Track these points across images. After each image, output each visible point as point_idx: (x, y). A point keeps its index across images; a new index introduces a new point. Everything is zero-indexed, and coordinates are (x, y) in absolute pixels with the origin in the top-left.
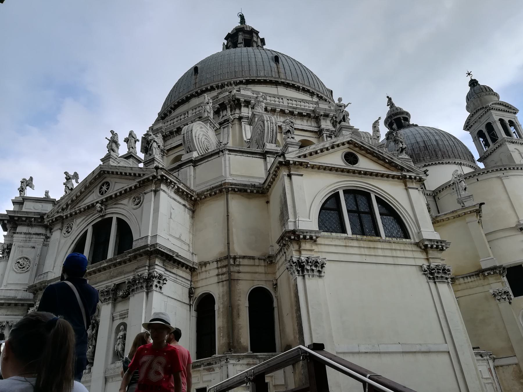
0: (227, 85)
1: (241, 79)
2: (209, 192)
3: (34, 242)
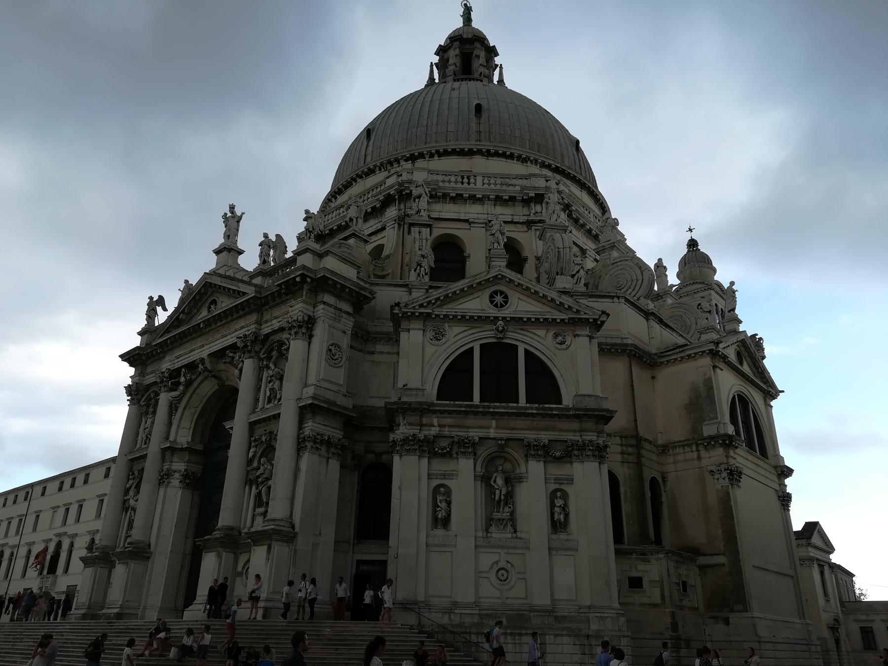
0: (531, 162)
1: (552, 162)
2: (608, 347)
3: (343, 323)
